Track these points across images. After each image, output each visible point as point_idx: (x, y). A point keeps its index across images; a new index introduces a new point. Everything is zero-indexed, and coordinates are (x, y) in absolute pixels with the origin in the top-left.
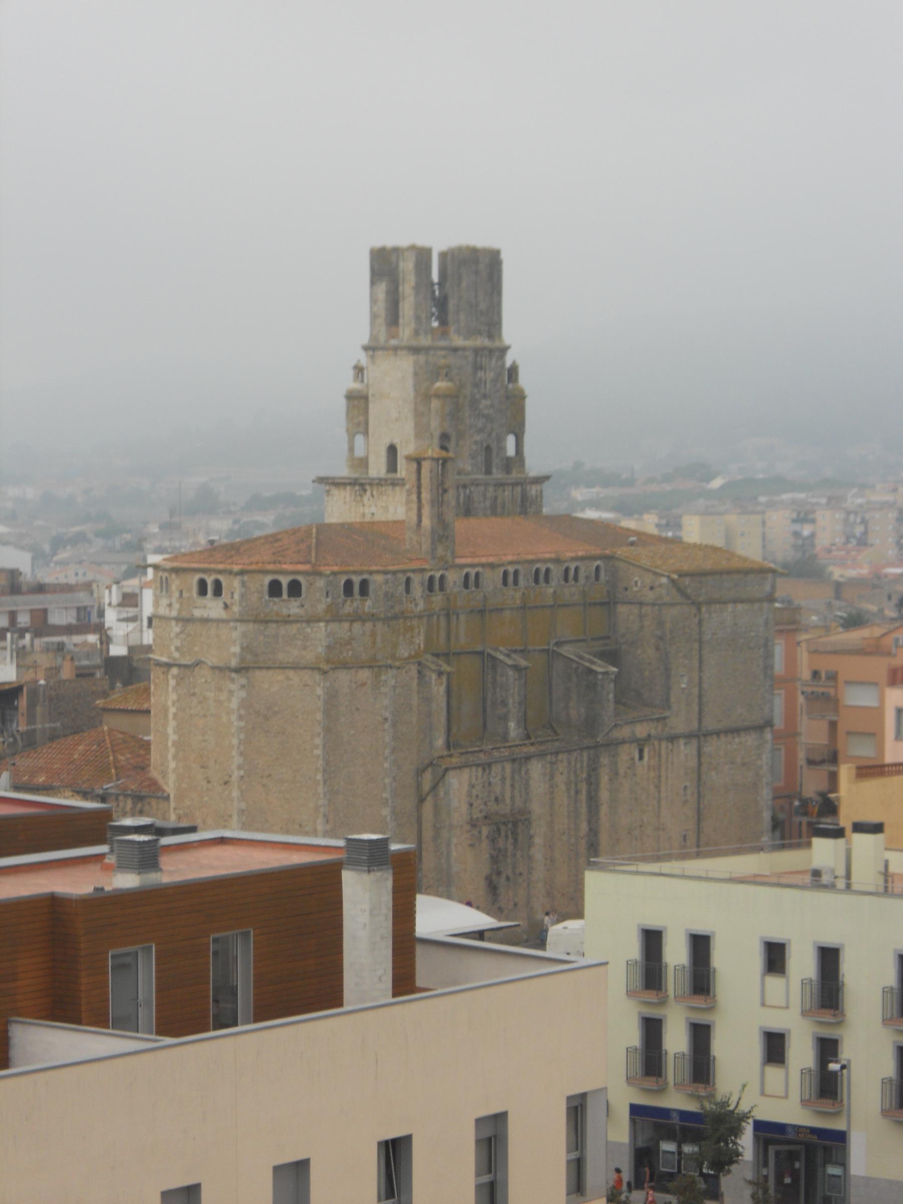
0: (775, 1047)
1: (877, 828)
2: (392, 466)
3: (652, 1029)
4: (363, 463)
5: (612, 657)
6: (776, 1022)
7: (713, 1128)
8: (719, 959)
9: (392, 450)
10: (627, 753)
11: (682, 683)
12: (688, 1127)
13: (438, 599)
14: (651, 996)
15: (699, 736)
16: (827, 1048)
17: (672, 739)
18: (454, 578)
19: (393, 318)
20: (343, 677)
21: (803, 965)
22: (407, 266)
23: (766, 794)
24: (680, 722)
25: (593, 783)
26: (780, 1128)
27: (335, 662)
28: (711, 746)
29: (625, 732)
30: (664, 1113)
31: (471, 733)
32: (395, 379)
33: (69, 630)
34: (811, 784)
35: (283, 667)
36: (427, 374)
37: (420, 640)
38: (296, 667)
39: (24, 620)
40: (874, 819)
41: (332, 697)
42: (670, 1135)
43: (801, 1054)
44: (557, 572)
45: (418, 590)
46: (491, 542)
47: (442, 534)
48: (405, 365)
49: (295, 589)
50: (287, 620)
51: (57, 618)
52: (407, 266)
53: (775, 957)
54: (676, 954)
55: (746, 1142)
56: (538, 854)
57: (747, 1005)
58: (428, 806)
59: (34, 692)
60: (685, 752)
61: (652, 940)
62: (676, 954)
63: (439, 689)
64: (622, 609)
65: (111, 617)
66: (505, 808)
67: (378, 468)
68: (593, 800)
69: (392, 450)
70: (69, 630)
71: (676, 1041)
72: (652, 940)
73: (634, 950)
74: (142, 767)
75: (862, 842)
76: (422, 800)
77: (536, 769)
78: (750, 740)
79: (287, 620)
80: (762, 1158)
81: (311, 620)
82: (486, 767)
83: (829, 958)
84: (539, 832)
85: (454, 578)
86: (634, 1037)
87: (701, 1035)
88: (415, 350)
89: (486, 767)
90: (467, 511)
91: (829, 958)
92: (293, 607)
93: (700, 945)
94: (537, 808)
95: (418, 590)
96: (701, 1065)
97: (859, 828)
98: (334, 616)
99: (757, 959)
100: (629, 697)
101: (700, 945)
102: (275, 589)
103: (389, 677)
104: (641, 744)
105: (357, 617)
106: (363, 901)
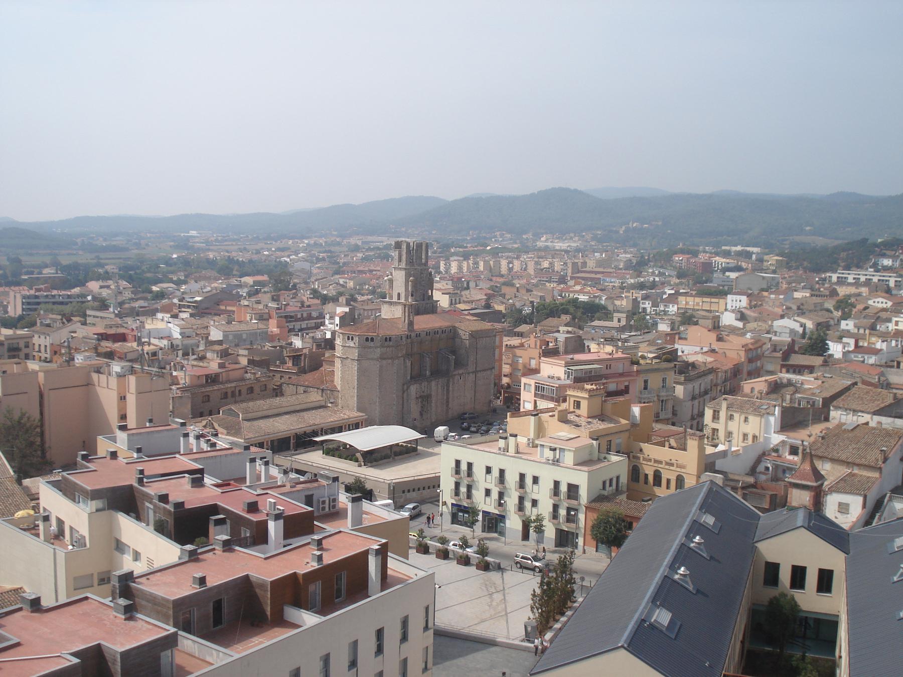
0: (488, 492)
1: (516, 436)
2: (399, 299)
3: (457, 485)
4: (391, 297)
5: (454, 352)
6: (489, 486)
7: (471, 511)
8: (475, 469)
9: (399, 294)
10: (457, 377)
11: (472, 358)
12: (465, 510)
13: (409, 340)
14: (457, 476)
15: (475, 372)
16: (501, 495)
17: (469, 373)
18: (413, 335)
19: (400, 260)
20: (384, 362)
21: (495, 473)
22: (404, 247)
23: (492, 385)
24: (471, 368)
25: (448, 386)
26: (489, 513)
27: (382, 358)
28: (479, 375)
29: (456, 372)
30: (460, 506)
31: (417, 377)
32: (399, 277)
33: (317, 318)
34: (505, 380)
35: (369, 359)
36: (408, 276)
37: (404, 352)
38: (372, 359)
39: (305, 315)
40: (515, 433)
41: (381, 367)
42: (461, 511)
43: (495, 495)
44: (440, 331)
45: (404, 339)
46: (424, 323)
47: (411, 324)
48: (403, 273)
49: (372, 340)
50: (370, 347)
51: (314, 314)
52: (404, 247)
53: (489, 470)
54: (464, 467)
55: (480, 517)
56: (433, 405)
57: (482, 481)
58: (405, 395)
59: (305, 354)
60: (472, 376)
61: (458, 463)
62: (464, 467)
63: (409, 364)
64: (457, 340)
65: (327, 322)
66: (425, 394)
67: (395, 299)
68: (448, 390)
69: (399, 294)
70: (317, 318)
71: (463, 490)
72: (458, 463)
73: (454, 465)
74: (333, 381)
75: (512, 440)
76: (404, 392)
77: (433, 383)
78: (489, 372)
79: (370, 347)
80: (484, 520)
81: (376, 347)
82: (421, 384)
83: (502, 472)
84: (434, 399)
85: (413, 335)
86: (453, 487)
87: (469, 488)
88: (405, 269)
89: (421, 384)
90: (418, 313)
91: (502, 472)
92: (372, 344)
93: (470, 465)
94: (433, 393)
95: (404, 339)
96: (469, 496)
97: (511, 435)
98: (382, 346)
99: (484, 471)
100: (459, 364)
101: (470, 465)
102: (367, 339)
103: (396, 361)
104: (460, 375)
105: (389, 346)
106: (373, 564)
